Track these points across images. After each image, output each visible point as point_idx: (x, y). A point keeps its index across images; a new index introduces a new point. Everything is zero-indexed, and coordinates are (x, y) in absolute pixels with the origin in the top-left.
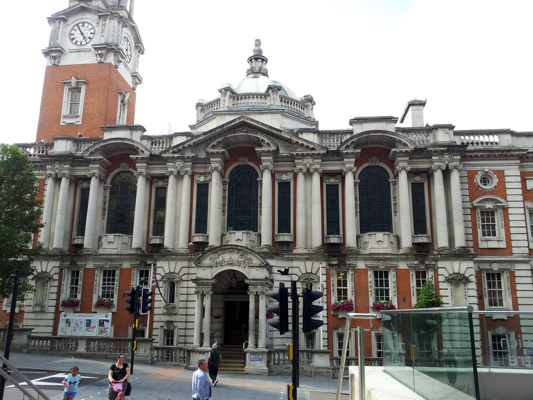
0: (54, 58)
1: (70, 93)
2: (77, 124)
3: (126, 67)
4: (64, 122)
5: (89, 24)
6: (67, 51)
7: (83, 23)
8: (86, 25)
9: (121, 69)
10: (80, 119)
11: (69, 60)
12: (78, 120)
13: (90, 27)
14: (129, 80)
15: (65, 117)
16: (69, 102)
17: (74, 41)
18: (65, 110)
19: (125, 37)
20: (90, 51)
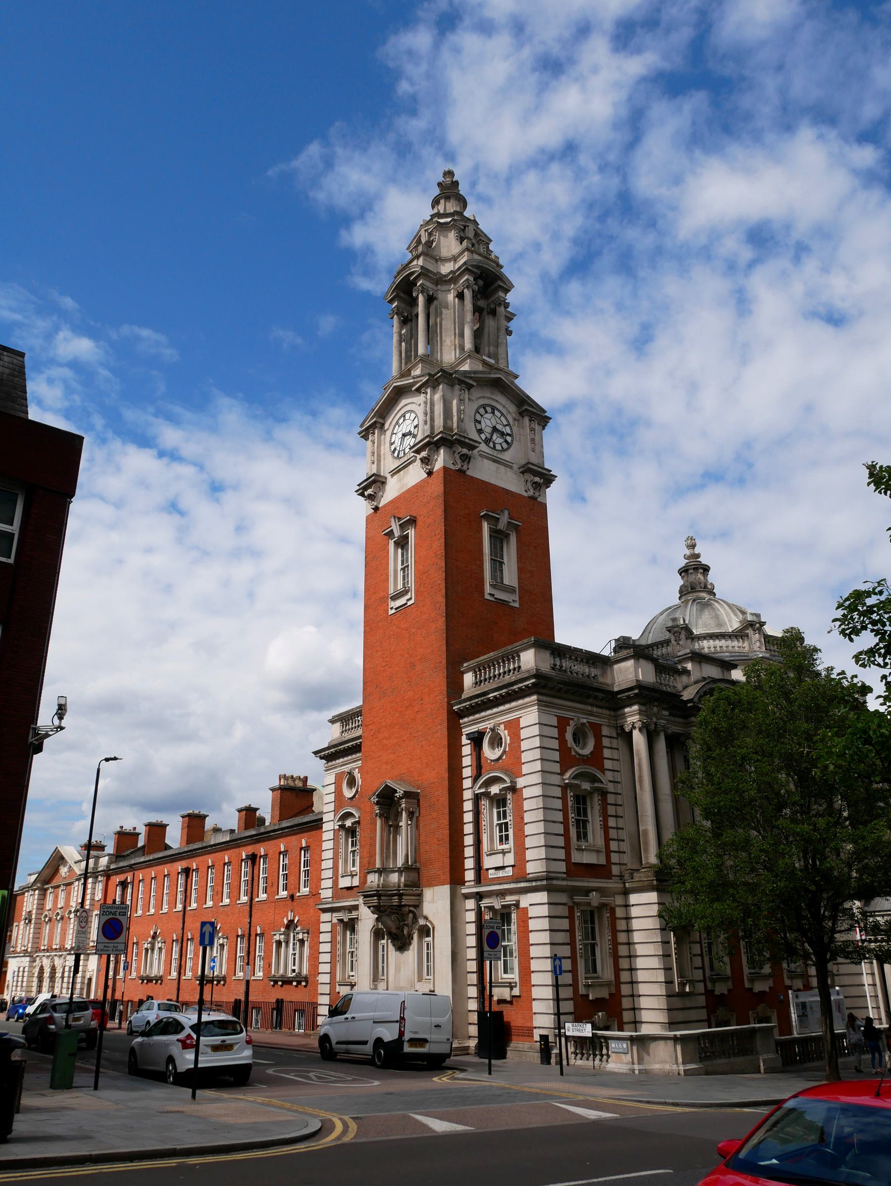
0: (371, 497)
1: (400, 551)
2: (410, 603)
3: (494, 461)
4: (392, 608)
5: (411, 411)
6: (389, 476)
7: (404, 416)
8: (407, 416)
9: (484, 470)
10: (412, 594)
11: (392, 490)
12: (408, 597)
13: (413, 416)
14: (511, 482)
15: (394, 598)
16: (400, 567)
17: (396, 454)
18: (395, 584)
19: (484, 407)
20: (414, 461)
